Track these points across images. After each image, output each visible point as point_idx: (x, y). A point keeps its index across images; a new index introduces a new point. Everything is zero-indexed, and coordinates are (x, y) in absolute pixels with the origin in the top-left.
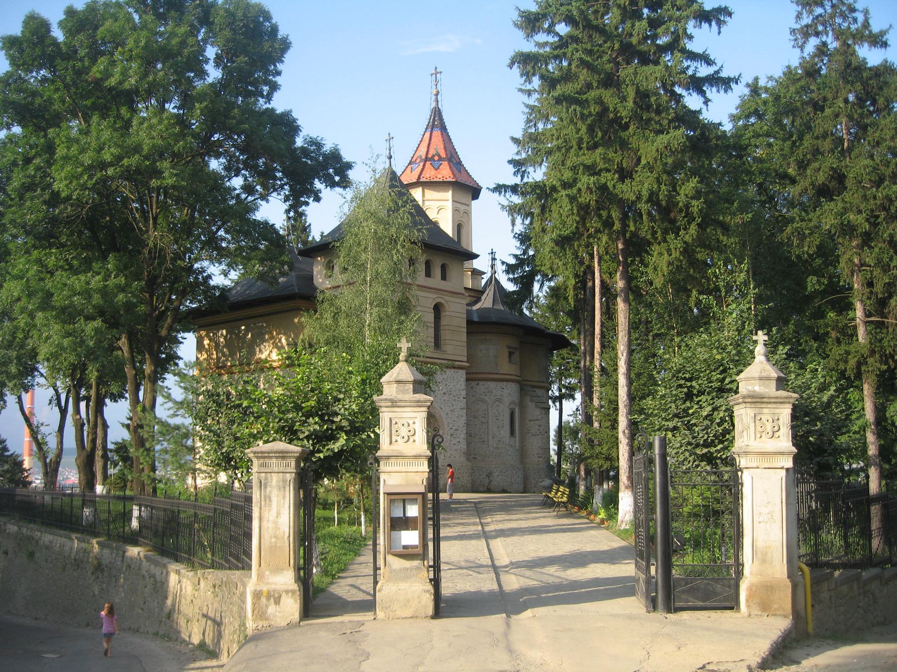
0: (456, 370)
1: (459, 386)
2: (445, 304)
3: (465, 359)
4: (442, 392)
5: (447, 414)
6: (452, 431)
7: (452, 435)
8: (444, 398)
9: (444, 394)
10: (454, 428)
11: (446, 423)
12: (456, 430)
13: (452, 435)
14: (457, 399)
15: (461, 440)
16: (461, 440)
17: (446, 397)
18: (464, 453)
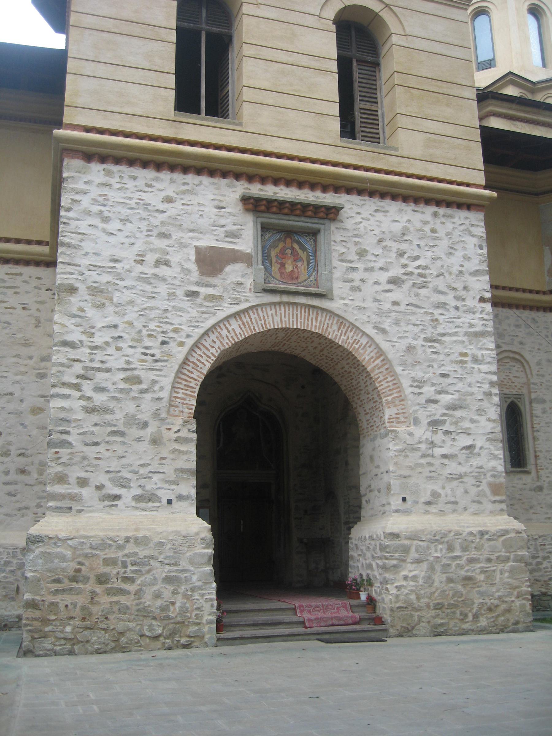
0: (442, 211)
1: (455, 261)
2: (386, 15)
3: (480, 178)
4: (384, 277)
5: (410, 349)
6: (437, 411)
7: (434, 424)
8: (396, 295)
9: (394, 281)
10: (446, 399)
11: (406, 383)
12: (454, 407)
13: (434, 424)
14: (454, 303)
15: (480, 442)
16: (480, 442)
17: (397, 295)
18: (495, 489)
